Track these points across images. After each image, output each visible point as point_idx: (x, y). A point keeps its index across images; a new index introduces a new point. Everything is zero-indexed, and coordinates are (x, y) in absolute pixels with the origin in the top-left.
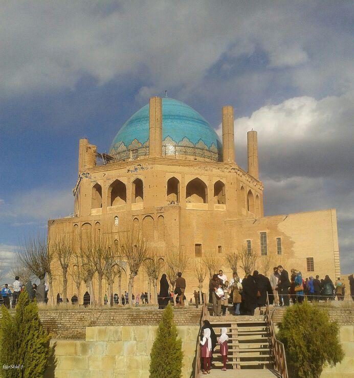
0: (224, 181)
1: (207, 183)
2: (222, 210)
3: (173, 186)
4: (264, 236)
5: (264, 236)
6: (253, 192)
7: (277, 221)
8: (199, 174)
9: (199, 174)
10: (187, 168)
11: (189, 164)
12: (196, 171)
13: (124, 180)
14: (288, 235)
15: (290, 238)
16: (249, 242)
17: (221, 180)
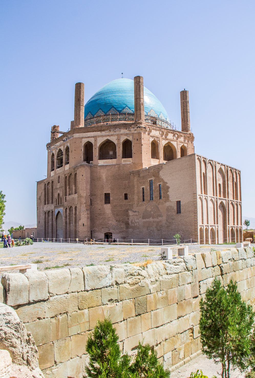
0: (130, 138)
1: (116, 142)
2: (128, 163)
3: (88, 147)
4: (151, 183)
5: (151, 183)
6: (174, 144)
7: (159, 168)
8: (108, 135)
9: (108, 135)
10: (99, 133)
11: (101, 129)
12: (107, 134)
13: (62, 148)
14: (165, 181)
15: (166, 183)
16: (143, 188)
17: (128, 138)
